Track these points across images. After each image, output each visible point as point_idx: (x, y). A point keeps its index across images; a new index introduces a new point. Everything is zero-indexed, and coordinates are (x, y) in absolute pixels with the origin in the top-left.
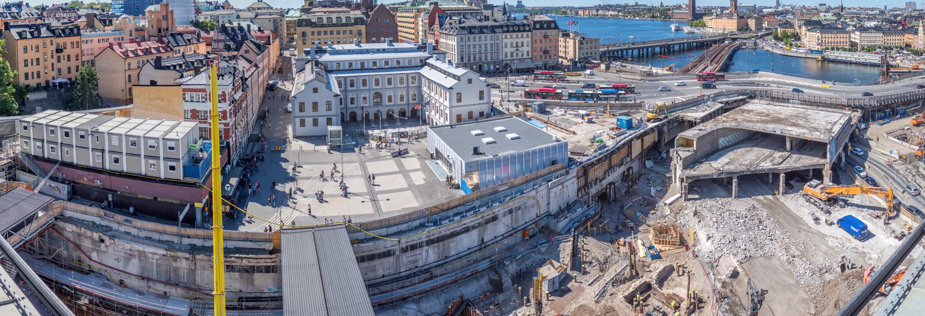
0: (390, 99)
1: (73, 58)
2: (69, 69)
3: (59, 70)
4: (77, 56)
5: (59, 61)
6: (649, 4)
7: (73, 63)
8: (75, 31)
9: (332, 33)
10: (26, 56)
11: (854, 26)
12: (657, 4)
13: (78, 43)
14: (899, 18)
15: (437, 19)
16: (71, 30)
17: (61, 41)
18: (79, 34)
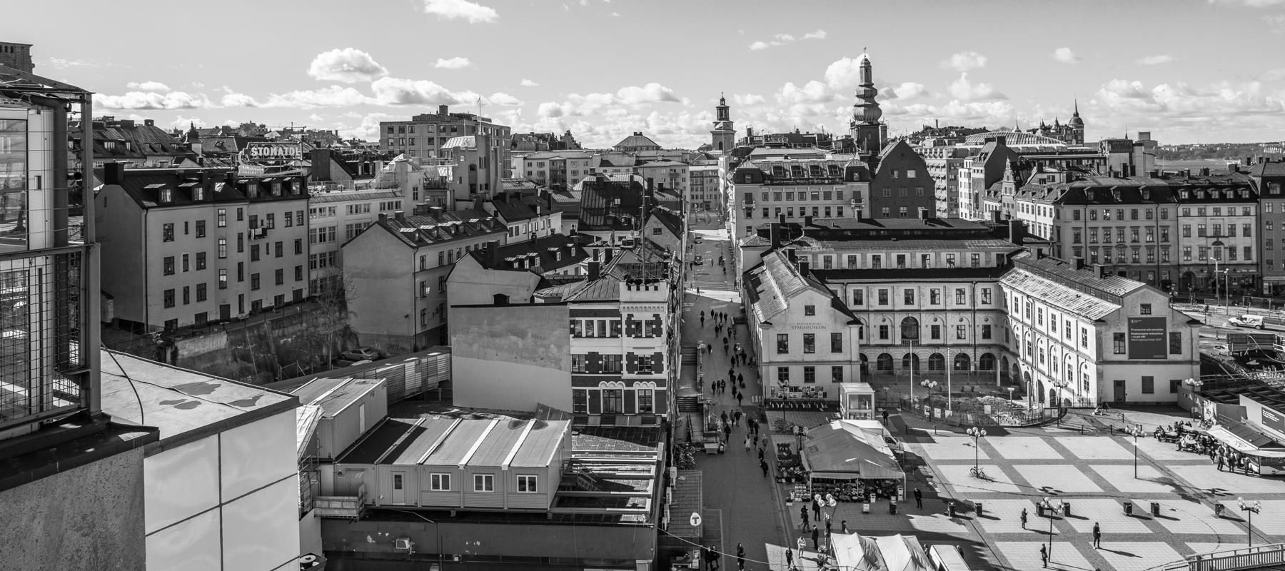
0: (935, 332)
1: (288, 249)
2: (279, 275)
3: (256, 280)
4: (298, 243)
5: (255, 256)
7: (290, 260)
8: (295, 188)
9: (827, 196)
10: (169, 249)
13: (301, 214)
15: (1008, 172)
16: (287, 186)
17: (261, 210)
18: (304, 195)
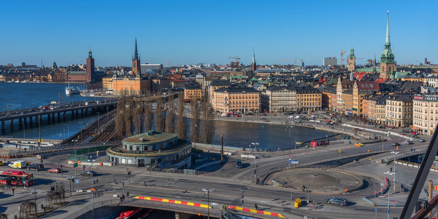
6: (39, 65)
11: (265, 85)
12: (50, 65)
14: (316, 76)
